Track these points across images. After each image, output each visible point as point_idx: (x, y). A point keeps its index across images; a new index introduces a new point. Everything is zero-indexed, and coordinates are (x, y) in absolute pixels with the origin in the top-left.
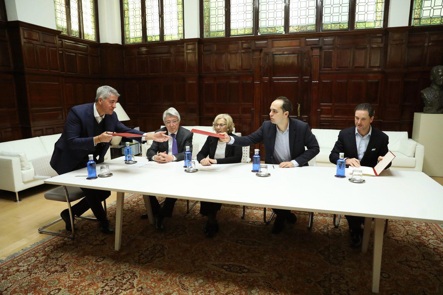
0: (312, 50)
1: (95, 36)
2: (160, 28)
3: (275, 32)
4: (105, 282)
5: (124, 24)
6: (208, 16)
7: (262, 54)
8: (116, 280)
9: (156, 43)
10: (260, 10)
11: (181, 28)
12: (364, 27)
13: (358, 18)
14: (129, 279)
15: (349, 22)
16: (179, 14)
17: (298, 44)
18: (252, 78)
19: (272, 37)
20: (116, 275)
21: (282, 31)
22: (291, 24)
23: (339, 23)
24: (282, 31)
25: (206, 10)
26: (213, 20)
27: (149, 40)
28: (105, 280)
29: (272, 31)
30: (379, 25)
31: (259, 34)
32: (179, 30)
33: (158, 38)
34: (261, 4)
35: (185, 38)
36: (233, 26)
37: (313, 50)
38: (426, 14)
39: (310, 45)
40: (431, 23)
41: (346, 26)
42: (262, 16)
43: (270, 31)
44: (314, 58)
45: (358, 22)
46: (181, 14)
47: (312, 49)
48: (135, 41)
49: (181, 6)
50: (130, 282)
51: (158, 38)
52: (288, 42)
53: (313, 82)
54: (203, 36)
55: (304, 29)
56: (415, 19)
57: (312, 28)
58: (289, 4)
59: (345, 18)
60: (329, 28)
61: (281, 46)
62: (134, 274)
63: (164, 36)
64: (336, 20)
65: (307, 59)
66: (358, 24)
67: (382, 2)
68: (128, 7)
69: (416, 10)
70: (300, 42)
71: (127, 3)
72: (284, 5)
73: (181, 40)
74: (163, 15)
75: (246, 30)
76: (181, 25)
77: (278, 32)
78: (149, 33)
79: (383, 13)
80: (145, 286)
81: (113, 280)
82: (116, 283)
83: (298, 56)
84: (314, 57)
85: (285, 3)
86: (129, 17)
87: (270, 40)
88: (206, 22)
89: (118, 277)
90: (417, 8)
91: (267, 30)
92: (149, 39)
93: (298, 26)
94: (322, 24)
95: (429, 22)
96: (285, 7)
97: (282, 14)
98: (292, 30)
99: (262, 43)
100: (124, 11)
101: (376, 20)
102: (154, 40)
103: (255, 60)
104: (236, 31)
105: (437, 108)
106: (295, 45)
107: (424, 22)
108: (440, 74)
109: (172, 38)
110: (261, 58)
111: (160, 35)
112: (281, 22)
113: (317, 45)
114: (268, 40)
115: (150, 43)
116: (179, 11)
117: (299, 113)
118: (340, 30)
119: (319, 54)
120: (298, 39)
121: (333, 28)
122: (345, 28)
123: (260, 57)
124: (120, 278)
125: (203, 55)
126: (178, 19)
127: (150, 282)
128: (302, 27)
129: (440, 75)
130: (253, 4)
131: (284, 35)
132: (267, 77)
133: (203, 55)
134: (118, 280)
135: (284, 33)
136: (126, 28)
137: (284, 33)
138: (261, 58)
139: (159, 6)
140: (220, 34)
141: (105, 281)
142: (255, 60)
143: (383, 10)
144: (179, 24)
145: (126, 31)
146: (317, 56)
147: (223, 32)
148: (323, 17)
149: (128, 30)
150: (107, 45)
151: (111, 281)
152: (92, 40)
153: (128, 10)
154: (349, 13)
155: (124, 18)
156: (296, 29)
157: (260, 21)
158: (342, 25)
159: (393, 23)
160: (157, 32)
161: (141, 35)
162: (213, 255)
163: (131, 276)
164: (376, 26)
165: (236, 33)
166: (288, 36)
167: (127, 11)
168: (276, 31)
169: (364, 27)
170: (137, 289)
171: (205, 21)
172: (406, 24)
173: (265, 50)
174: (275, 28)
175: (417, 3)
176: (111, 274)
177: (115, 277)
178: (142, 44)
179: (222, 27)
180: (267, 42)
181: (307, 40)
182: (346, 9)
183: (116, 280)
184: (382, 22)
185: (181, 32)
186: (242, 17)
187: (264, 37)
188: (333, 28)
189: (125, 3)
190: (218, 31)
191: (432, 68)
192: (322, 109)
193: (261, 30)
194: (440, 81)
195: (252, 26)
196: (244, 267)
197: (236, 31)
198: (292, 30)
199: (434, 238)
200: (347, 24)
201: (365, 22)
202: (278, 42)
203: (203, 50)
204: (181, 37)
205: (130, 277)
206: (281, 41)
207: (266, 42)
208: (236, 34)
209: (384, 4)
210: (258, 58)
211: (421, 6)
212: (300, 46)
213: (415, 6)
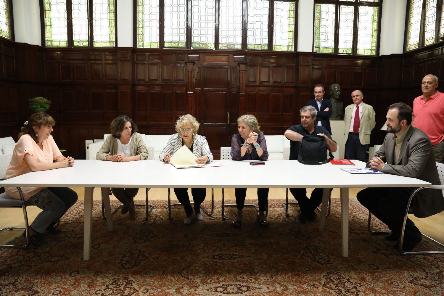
0: (239, 66)
1: (10, 34)
2: (88, 33)
3: (206, 48)
4: (100, 293)
5: (45, 24)
6: (142, 27)
7: (195, 66)
8: (111, 289)
9: (85, 48)
10: (192, 27)
11: (113, 36)
12: (280, 49)
13: (275, 42)
14: (126, 285)
15: (268, 44)
16: (111, 22)
17: (227, 60)
18: (185, 89)
19: (204, 52)
20: (107, 284)
21: (212, 47)
22: (220, 42)
23: (261, 45)
24: (212, 47)
25: (139, 21)
26: (146, 32)
27: (76, 45)
28: (97, 291)
29: (203, 46)
30: (291, 49)
31: (192, 48)
32: (110, 38)
33: (86, 44)
34: (194, 21)
35: (119, 46)
36: (167, 39)
37: (240, 66)
38: (322, 44)
39: (238, 61)
40: (327, 52)
41: (266, 48)
42: (194, 32)
43: (202, 46)
44: (241, 72)
45: (275, 45)
46: (113, 22)
47: (239, 64)
48: (58, 45)
49: (112, 14)
50: (128, 288)
51: (86, 44)
52: (219, 58)
54: (136, 46)
55: (232, 47)
56: (316, 47)
57: (239, 47)
58: (219, 24)
59: (266, 41)
60: (253, 48)
61: (213, 60)
62: (128, 279)
63: (93, 42)
64: (258, 41)
65: (234, 73)
66: (275, 47)
67: (293, 32)
68: (50, 7)
69: (316, 41)
70: (229, 59)
71: (49, 3)
72: (214, 24)
73: (114, 47)
74: (93, 21)
75: (180, 44)
76: (113, 33)
77: (209, 48)
78: (76, 38)
79: (293, 40)
80: (149, 288)
81: (107, 290)
82: (113, 291)
84: (240, 71)
85: (215, 22)
86: (51, 19)
87: (203, 54)
88: (139, 32)
89: (111, 286)
90: (316, 39)
91: (199, 45)
92: (76, 44)
93: (226, 44)
94: (247, 44)
95: (325, 51)
96: (215, 26)
97: (213, 33)
98: (221, 47)
99: (194, 56)
100: (45, 11)
101: (289, 45)
102: (81, 45)
103: (189, 72)
104: (170, 44)
105: (336, 116)
106: (224, 60)
107: (322, 51)
108: (337, 90)
109: (103, 45)
111: (88, 41)
112: (212, 40)
113: (243, 61)
114: (200, 55)
115: (78, 48)
116: (111, 18)
117: (229, 120)
118: (262, 50)
120: (226, 55)
121: (256, 48)
122: (265, 49)
124: (114, 286)
126: (110, 27)
127: (152, 283)
128: (230, 45)
129: (337, 91)
130: (186, 20)
131: (214, 51)
133: (136, 65)
134: (114, 288)
135: (214, 49)
136: (47, 29)
137: (214, 49)
138: (193, 70)
139: (88, 11)
140: (154, 45)
141: (98, 292)
143: (294, 38)
144: (111, 32)
145: (47, 33)
146: (244, 71)
147: (157, 44)
148: (248, 38)
149: (50, 32)
150: (25, 46)
151: (106, 291)
152: (6, 38)
153: (50, 10)
154: (268, 37)
155: (45, 19)
156: (225, 47)
157: (192, 37)
158: (263, 47)
159: (301, 49)
160: (86, 37)
161: (67, 39)
162: (198, 249)
163: (125, 282)
164: (289, 50)
165: (170, 46)
166: (218, 52)
167: (49, 12)
168: (207, 47)
169: (280, 49)
170: (141, 291)
171: (139, 31)
172: (311, 51)
173: (196, 62)
174: (207, 44)
175: (316, 35)
176: (99, 284)
177: (107, 286)
178: (67, 48)
179: (157, 39)
180: (199, 56)
181: (234, 56)
182: (266, 34)
183: (111, 289)
184: (293, 47)
185: (113, 39)
186: (175, 31)
187: (197, 51)
188: (256, 48)
189: (46, 3)
190: (151, 42)
191: (330, 86)
193: (193, 44)
194: (336, 95)
195: (185, 41)
196: (219, 260)
197: (170, 44)
198: (221, 47)
199: (361, 213)
200: (267, 46)
201: (281, 46)
202: (209, 56)
203: (137, 60)
204: (112, 45)
205: (125, 283)
206: (212, 56)
207: (198, 56)
208: (170, 46)
209: (294, 33)
210: (192, 70)
211: (319, 38)
212: (228, 61)
213: (315, 37)
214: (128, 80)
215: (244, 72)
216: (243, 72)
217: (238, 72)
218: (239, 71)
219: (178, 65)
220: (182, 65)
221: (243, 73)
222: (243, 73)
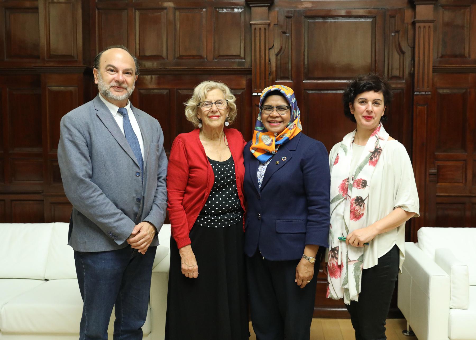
44: (420, 27)
53: (418, 93)
83: (374, 24)
84: (417, 25)
103: (255, 29)
110: (272, 25)
119: (431, 18)
123: (269, 22)
125: (97, 11)
132: (288, 78)
133: (97, 11)
138: (269, 24)
142: (255, 29)
146: (427, 25)
192: (439, 168)
210: (265, 24)
214: (71, 56)
215: (429, 27)
216: (425, 27)
217: (410, 27)
218: (414, 24)
219: (225, 10)
220: (236, 10)
221: (427, 28)
222: (427, 28)
